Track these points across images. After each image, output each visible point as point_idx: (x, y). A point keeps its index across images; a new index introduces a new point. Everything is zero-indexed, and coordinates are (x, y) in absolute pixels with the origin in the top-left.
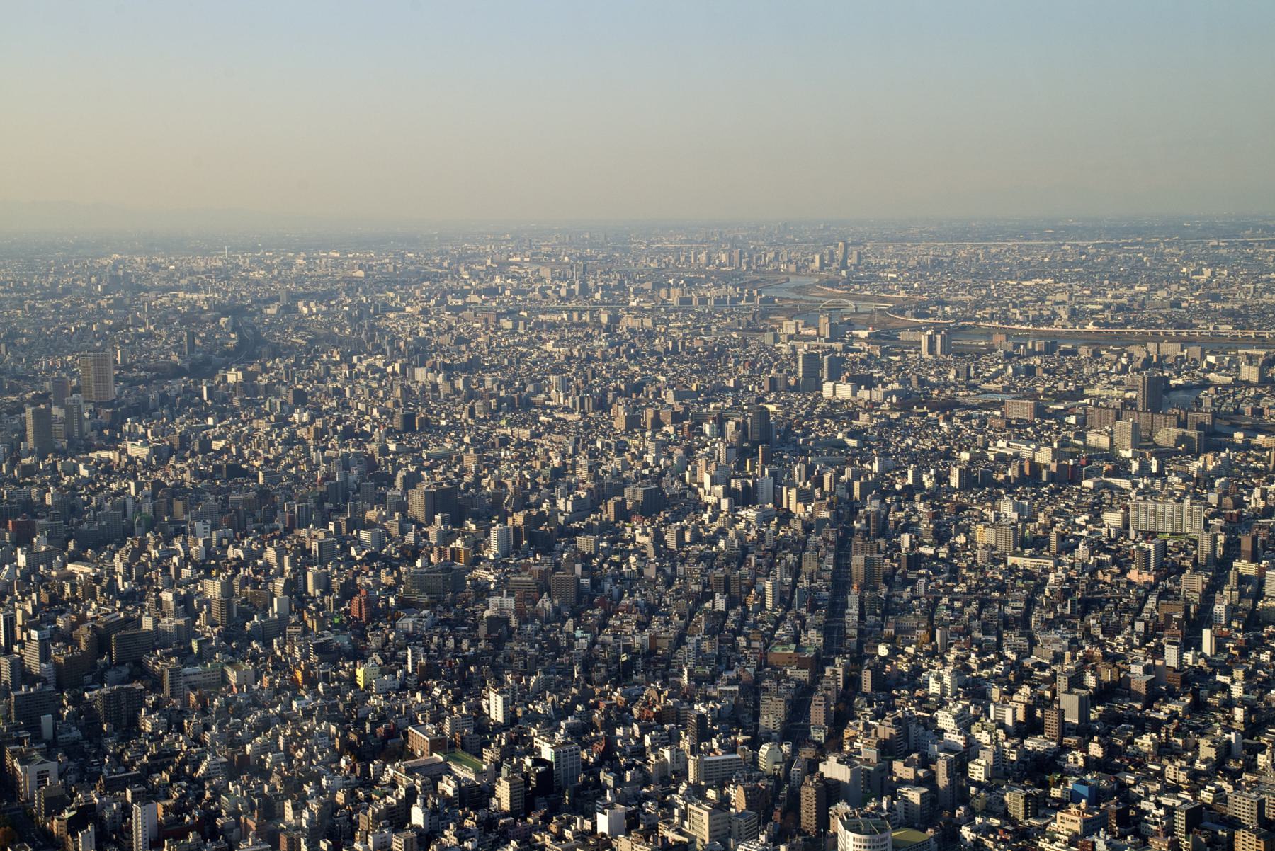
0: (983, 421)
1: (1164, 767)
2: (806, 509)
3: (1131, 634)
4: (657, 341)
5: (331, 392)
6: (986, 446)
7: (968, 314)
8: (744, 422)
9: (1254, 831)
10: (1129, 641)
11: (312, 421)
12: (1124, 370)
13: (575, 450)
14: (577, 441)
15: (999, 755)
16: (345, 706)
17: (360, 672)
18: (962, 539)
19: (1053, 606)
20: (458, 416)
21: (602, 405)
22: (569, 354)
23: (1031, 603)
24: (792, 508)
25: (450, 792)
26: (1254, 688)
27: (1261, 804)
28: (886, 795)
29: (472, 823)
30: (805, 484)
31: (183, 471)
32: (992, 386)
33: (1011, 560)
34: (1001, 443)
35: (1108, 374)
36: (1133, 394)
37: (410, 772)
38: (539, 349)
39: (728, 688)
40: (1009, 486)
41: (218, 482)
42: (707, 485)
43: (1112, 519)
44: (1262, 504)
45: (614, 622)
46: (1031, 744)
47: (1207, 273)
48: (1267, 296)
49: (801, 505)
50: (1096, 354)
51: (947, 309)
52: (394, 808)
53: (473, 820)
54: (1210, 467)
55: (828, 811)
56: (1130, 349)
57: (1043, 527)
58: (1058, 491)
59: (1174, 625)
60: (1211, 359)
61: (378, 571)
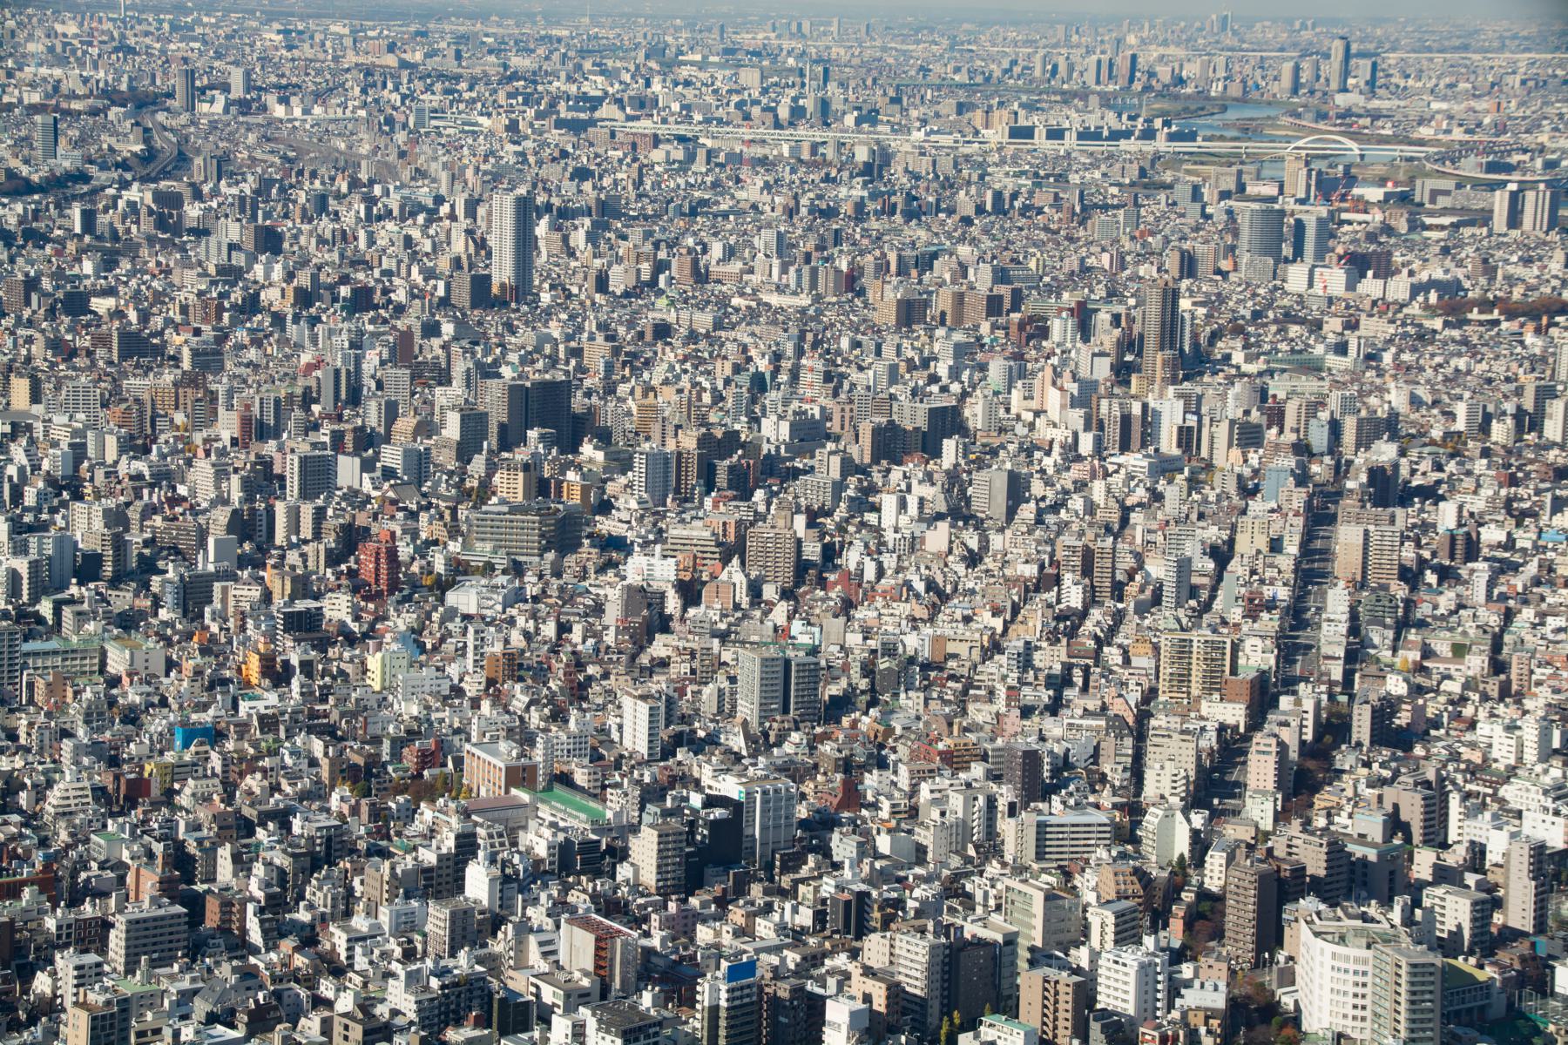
2: (1246, 461)
4: (962, 193)
5: (328, 235)
8: (1131, 320)
11: (290, 276)
13: (800, 352)
14: (802, 337)
16: (342, 715)
17: (374, 662)
20: (575, 290)
21: (851, 283)
22: (792, 204)
24: (1219, 460)
25: (541, 850)
28: (1400, 894)
29: (583, 896)
30: (1247, 413)
31: (29, 340)
37: (466, 814)
38: (733, 197)
39: (1085, 722)
41: (101, 363)
42: (1054, 412)
45: (861, 613)
49: (1236, 453)
52: (430, 870)
53: (584, 891)
55: (1280, 912)
61: (413, 515)
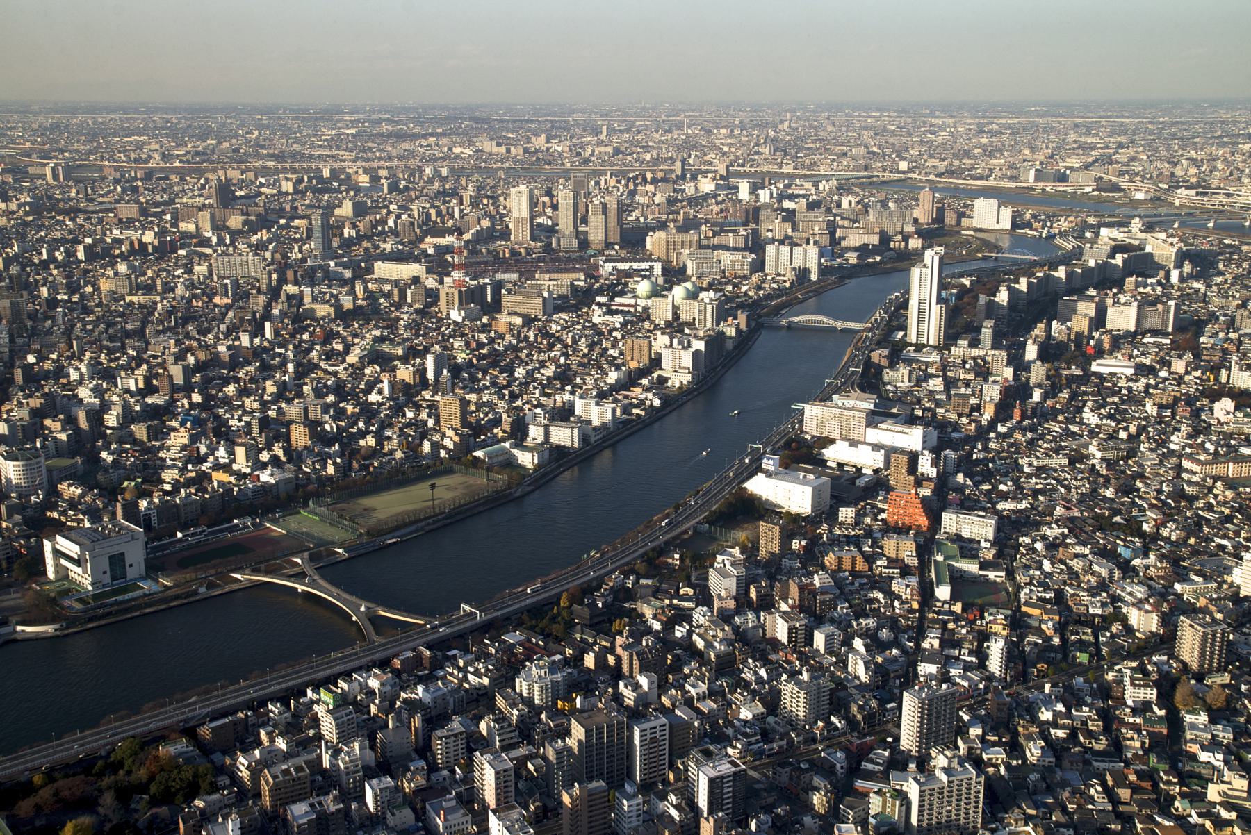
0: (101, 221)
1: (243, 402)
3: (217, 333)
6: (105, 234)
7: (84, 157)
9: (302, 423)
10: (216, 337)
12: (203, 187)
15: (126, 407)
18: (89, 289)
19: (162, 322)
23: (145, 322)
26: (299, 353)
27: (306, 410)
32: (105, 199)
33: (128, 299)
34: (116, 232)
35: (192, 190)
36: (211, 201)
40: (124, 257)
43: (200, 270)
44: (299, 256)
46: (149, 400)
47: (256, 133)
48: (295, 145)
50: (182, 179)
51: (66, 154)
54: (265, 238)
56: (207, 175)
57: (152, 278)
58: (162, 258)
59: (246, 323)
60: (263, 180)
